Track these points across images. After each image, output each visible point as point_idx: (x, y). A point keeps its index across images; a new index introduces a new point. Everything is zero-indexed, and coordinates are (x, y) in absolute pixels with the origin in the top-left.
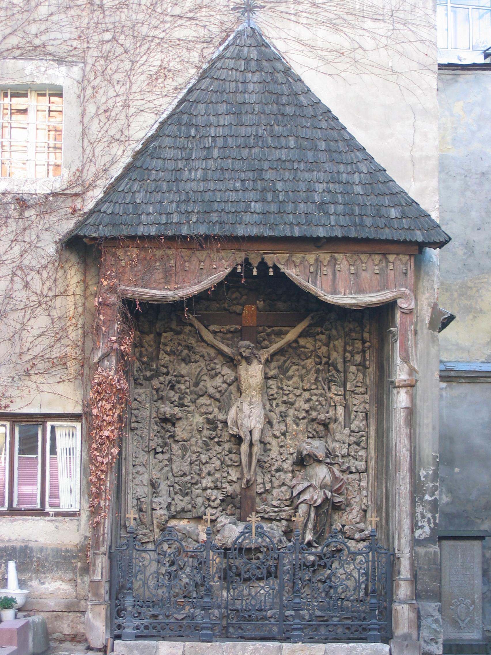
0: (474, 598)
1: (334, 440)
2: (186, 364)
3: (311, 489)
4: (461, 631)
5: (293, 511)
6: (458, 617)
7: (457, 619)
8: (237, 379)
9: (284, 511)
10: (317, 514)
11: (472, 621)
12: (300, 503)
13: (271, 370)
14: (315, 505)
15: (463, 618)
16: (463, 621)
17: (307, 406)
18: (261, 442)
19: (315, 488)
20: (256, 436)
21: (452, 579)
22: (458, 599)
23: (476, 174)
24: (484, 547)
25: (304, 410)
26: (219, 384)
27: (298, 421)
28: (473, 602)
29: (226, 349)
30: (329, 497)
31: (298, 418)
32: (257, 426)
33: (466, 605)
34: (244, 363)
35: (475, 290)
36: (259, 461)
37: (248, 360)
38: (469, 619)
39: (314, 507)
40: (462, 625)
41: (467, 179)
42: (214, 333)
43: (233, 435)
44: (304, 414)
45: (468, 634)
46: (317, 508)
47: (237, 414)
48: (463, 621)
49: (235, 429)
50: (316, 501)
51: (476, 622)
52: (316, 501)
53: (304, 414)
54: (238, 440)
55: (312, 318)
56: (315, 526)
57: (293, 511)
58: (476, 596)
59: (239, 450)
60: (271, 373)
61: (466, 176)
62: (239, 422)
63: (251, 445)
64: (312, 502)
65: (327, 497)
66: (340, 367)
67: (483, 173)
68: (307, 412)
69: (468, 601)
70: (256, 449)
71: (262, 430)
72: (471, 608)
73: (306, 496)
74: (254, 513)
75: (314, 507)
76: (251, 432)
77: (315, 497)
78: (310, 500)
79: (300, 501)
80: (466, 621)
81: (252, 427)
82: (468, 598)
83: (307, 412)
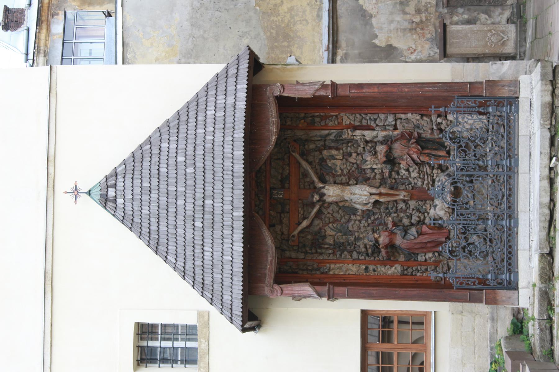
0: (487, 30)
1: (377, 137)
2: (326, 238)
3: (411, 152)
4: (510, 38)
5: (426, 165)
6: (500, 41)
7: (502, 42)
8: (337, 203)
9: (426, 171)
10: (427, 148)
11: (503, 32)
12: (420, 160)
13: (330, 181)
14: (421, 150)
15: (501, 38)
16: (503, 38)
17: (354, 155)
18: (378, 188)
19: (409, 150)
20: (374, 191)
21: (474, 45)
22: (487, 42)
23: (192, 30)
24: (451, 23)
25: (356, 157)
26: (339, 216)
27: (364, 161)
28: (490, 31)
29: (315, 210)
30: (415, 140)
31: (362, 161)
32: (367, 190)
33: (491, 36)
34: (325, 198)
35: (272, 31)
36: (392, 188)
37: (322, 195)
38: (501, 34)
39: (422, 150)
40: (506, 38)
41: (195, 36)
42: (304, 218)
43: (373, 206)
44: (360, 157)
45: (512, 34)
46: (423, 148)
47: (359, 204)
48: (503, 38)
49: (370, 205)
50: (418, 150)
51: (504, 28)
52: (418, 150)
53: (360, 157)
54: (376, 203)
55: (293, 152)
56: (436, 149)
57: (426, 165)
58: (485, 29)
59: (384, 203)
60: (332, 180)
61: (194, 37)
62: (365, 202)
63: (380, 194)
64: (419, 152)
65: (415, 142)
66: (326, 132)
67: (192, 25)
68: (358, 154)
69: (489, 34)
70: (383, 190)
71: (371, 186)
72: (494, 32)
73: (415, 156)
74: (428, 192)
75: (422, 150)
76: (371, 194)
77: (415, 150)
78: (417, 154)
79: (418, 160)
80: (503, 35)
81: (368, 194)
82: (487, 34)
83: (358, 154)
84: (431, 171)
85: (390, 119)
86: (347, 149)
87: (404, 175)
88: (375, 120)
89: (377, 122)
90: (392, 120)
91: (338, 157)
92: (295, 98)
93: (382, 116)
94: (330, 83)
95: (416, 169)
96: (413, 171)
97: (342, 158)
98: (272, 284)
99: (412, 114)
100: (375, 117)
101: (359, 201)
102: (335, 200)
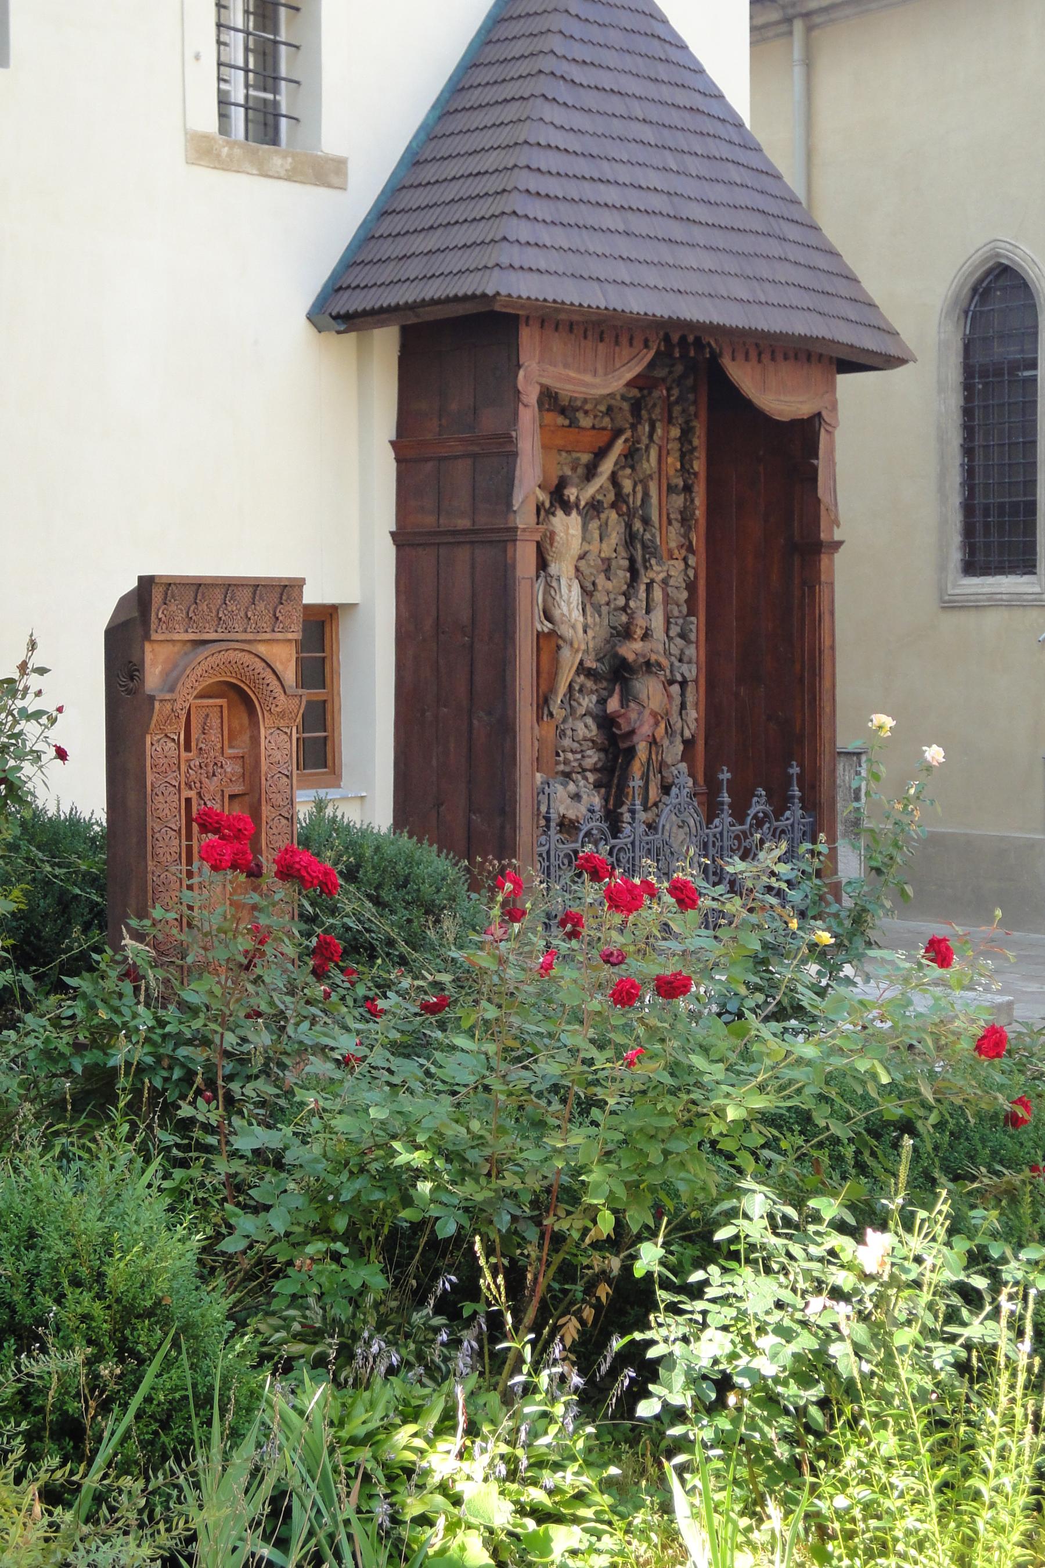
49: (550, 625)
84: (588, 767)
85: (690, 671)
86: (620, 568)
87: (580, 704)
88: (683, 636)
89: (679, 641)
90: (687, 674)
91: (604, 546)
92: (817, 458)
93: (691, 651)
94: (837, 538)
95: (590, 731)
96: (586, 726)
97: (603, 555)
98: (544, 381)
99: (696, 720)
100: (693, 637)
101: (558, 598)
102: (557, 538)
